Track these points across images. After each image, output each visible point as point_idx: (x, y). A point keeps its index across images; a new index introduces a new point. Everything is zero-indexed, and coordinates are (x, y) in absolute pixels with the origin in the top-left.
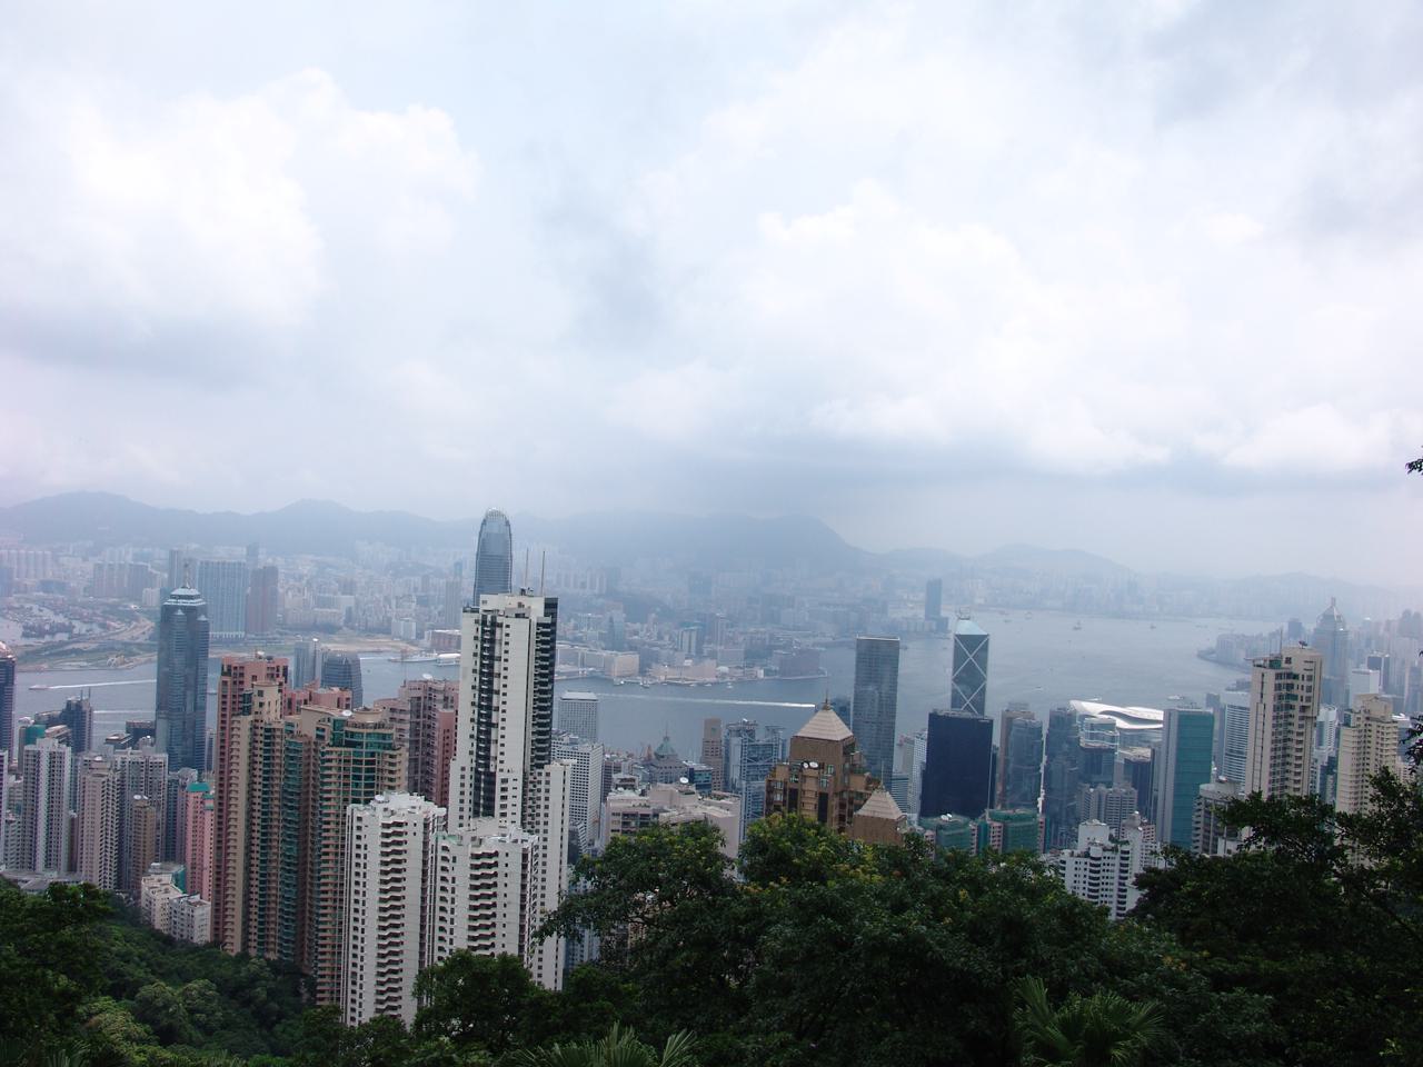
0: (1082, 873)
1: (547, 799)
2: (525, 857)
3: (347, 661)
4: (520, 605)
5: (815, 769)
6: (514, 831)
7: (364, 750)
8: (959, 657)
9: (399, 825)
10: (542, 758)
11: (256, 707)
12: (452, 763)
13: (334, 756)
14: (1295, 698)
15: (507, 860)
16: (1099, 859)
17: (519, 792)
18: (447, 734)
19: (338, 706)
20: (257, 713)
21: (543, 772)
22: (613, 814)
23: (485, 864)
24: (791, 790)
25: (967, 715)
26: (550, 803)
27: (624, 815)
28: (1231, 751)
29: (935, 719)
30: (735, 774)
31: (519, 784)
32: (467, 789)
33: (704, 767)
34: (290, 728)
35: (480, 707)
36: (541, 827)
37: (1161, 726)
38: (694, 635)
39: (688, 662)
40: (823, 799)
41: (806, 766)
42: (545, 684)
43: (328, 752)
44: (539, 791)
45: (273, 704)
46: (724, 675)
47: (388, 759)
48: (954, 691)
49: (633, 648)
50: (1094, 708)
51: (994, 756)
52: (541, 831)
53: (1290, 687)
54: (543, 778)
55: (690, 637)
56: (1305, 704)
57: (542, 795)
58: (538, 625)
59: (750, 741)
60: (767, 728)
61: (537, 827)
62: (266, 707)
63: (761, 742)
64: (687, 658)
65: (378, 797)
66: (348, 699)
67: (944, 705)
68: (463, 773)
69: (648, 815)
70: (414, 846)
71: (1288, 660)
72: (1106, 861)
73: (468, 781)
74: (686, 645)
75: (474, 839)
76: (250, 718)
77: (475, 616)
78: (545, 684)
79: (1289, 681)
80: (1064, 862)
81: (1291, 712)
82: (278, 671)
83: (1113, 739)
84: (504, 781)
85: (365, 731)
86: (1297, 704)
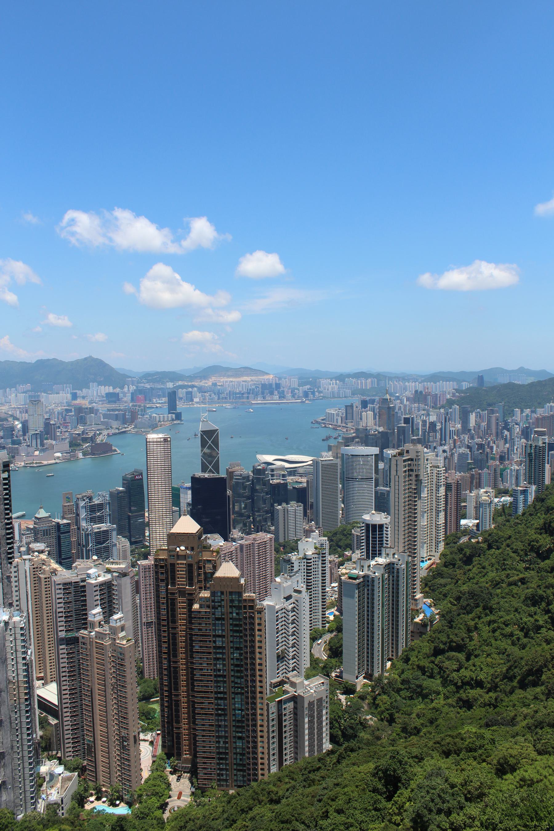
0: (302, 568)
14: (412, 470)
16: (311, 559)
24: (171, 564)
27: (65, 584)
28: (349, 478)
29: (195, 480)
30: (83, 524)
33: (65, 521)
38: (38, 436)
39: (37, 453)
40: (190, 566)
41: (178, 549)
42: (8, 514)
46: (58, 458)
50: (269, 458)
53: (410, 465)
59: (90, 503)
63: (96, 503)
64: (35, 451)
71: (408, 452)
72: (314, 560)
79: (409, 462)
80: (293, 563)
81: (410, 478)
86: (414, 474)
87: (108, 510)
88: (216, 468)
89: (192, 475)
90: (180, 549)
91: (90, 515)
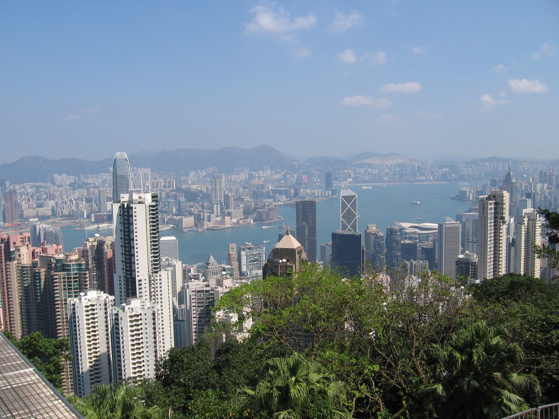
1: (161, 287)
2: (154, 314)
3: (55, 232)
4: (140, 198)
6: (148, 304)
7: (72, 272)
8: (344, 206)
9: (93, 305)
10: (157, 268)
11: (17, 257)
12: (114, 274)
13: (57, 277)
15: (146, 317)
17: (148, 285)
18: (110, 261)
19: (56, 253)
20: (18, 260)
21: (158, 275)
22: (193, 291)
23: (136, 318)
25: (350, 233)
26: (162, 289)
27: (198, 291)
29: (335, 236)
30: (244, 269)
31: (147, 281)
32: (123, 286)
34: (35, 266)
35: (125, 247)
36: (159, 300)
37: (437, 231)
38: (219, 205)
41: (281, 261)
42: (155, 234)
43: (56, 275)
44: (157, 284)
46: (234, 223)
48: (342, 222)
49: (190, 214)
50: (405, 225)
51: (363, 250)
52: (159, 302)
54: (158, 278)
55: (217, 206)
56: (501, 216)
57: (158, 285)
58: (150, 206)
61: (157, 301)
64: (216, 217)
65: (82, 294)
66: (60, 249)
68: (120, 279)
69: (208, 291)
70: (100, 314)
71: (494, 197)
73: (123, 282)
74: (215, 211)
75: (129, 309)
76: (15, 262)
78: (155, 234)
82: (25, 239)
83: (416, 239)
84: (140, 281)
85: (71, 263)
87: (264, 259)
88: (354, 227)
89: (333, 232)
90: (282, 261)
91: (250, 262)
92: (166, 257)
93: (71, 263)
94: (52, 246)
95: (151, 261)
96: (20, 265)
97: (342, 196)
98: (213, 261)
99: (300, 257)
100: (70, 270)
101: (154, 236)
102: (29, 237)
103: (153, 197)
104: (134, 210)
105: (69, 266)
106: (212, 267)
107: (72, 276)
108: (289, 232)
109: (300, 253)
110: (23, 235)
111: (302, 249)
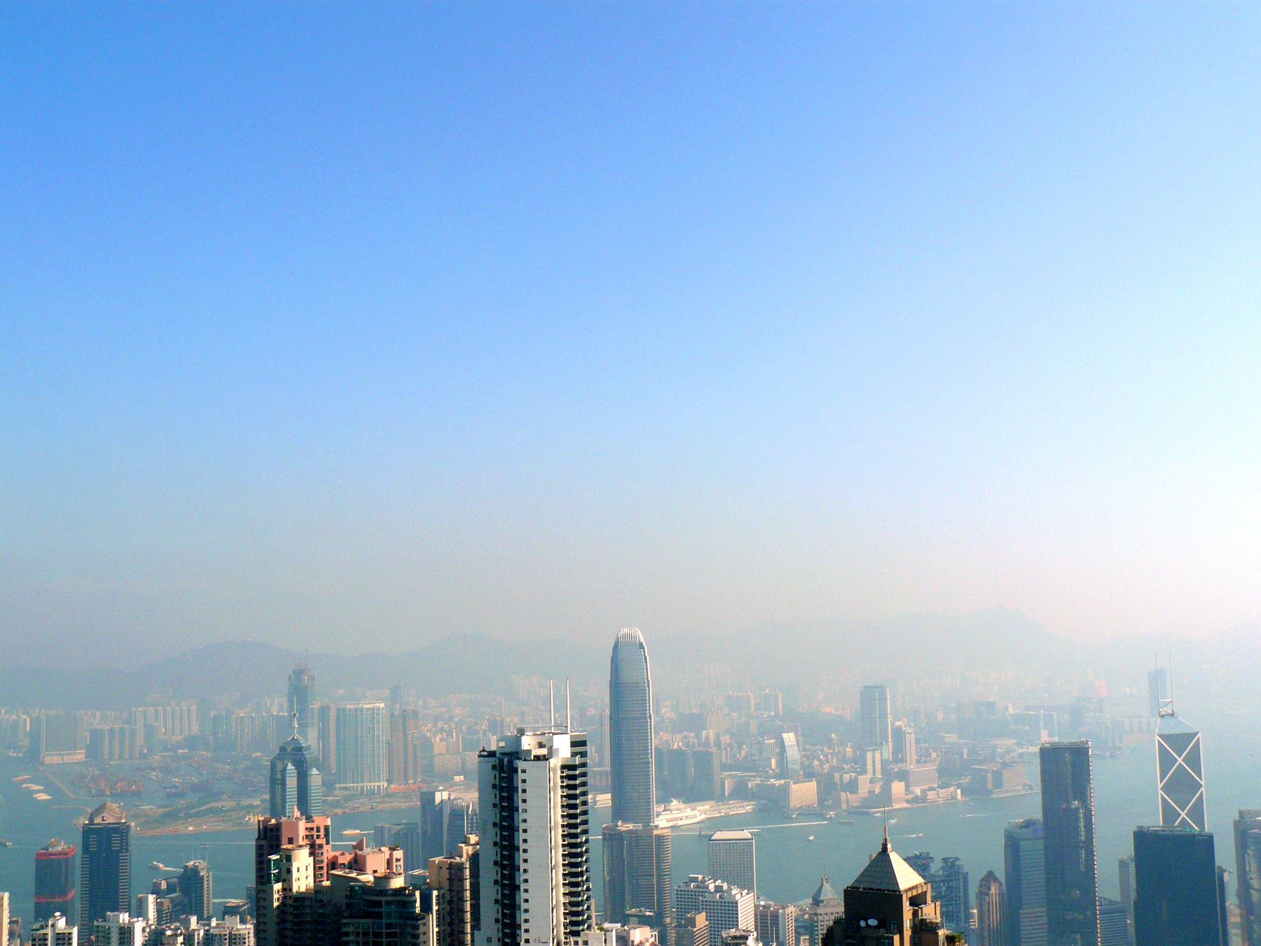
5: (875, 927)
7: (384, 921)
8: (1166, 761)
13: (351, 929)
21: (580, 940)
41: (863, 924)
45: (303, 870)
46: (914, 800)
47: (409, 929)
49: (809, 775)
60: (945, 860)
62: (295, 875)
66: (398, 860)
67: (1156, 821)
74: (870, 767)
77: (495, 758)
85: (383, 899)
87: (962, 895)
89: (1135, 829)
92: (718, 883)
93: (383, 899)
94: (380, 850)
95: (564, 903)
96: (288, 894)
97: (1160, 736)
98: (830, 896)
99: (915, 914)
100: (379, 916)
101: (573, 841)
102: (326, 828)
103: (574, 744)
104: (521, 776)
105: (379, 904)
106: (829, 910)
107: (384, 931)
108: (889, 846)
109: (917, 901)
110: (313, 822)
111: (926, 892)
